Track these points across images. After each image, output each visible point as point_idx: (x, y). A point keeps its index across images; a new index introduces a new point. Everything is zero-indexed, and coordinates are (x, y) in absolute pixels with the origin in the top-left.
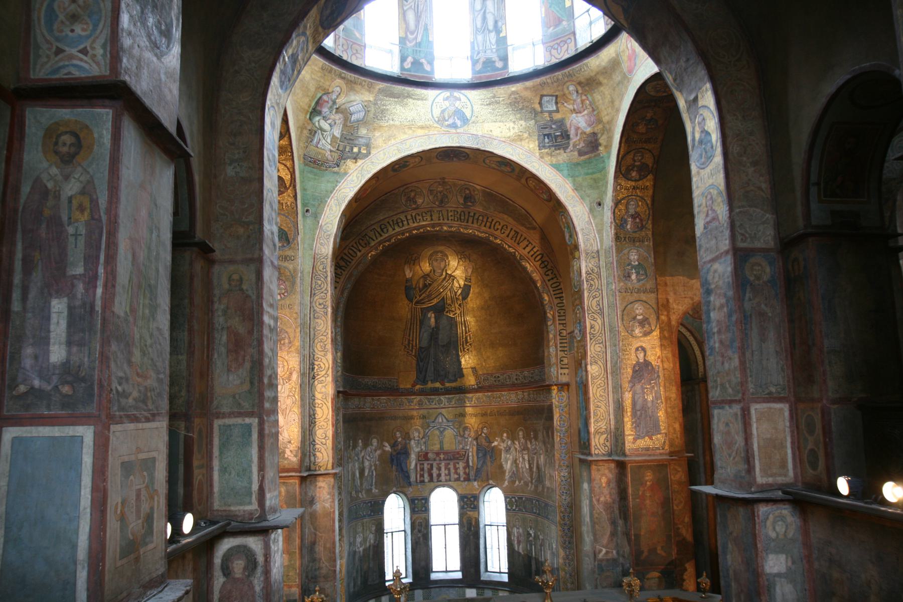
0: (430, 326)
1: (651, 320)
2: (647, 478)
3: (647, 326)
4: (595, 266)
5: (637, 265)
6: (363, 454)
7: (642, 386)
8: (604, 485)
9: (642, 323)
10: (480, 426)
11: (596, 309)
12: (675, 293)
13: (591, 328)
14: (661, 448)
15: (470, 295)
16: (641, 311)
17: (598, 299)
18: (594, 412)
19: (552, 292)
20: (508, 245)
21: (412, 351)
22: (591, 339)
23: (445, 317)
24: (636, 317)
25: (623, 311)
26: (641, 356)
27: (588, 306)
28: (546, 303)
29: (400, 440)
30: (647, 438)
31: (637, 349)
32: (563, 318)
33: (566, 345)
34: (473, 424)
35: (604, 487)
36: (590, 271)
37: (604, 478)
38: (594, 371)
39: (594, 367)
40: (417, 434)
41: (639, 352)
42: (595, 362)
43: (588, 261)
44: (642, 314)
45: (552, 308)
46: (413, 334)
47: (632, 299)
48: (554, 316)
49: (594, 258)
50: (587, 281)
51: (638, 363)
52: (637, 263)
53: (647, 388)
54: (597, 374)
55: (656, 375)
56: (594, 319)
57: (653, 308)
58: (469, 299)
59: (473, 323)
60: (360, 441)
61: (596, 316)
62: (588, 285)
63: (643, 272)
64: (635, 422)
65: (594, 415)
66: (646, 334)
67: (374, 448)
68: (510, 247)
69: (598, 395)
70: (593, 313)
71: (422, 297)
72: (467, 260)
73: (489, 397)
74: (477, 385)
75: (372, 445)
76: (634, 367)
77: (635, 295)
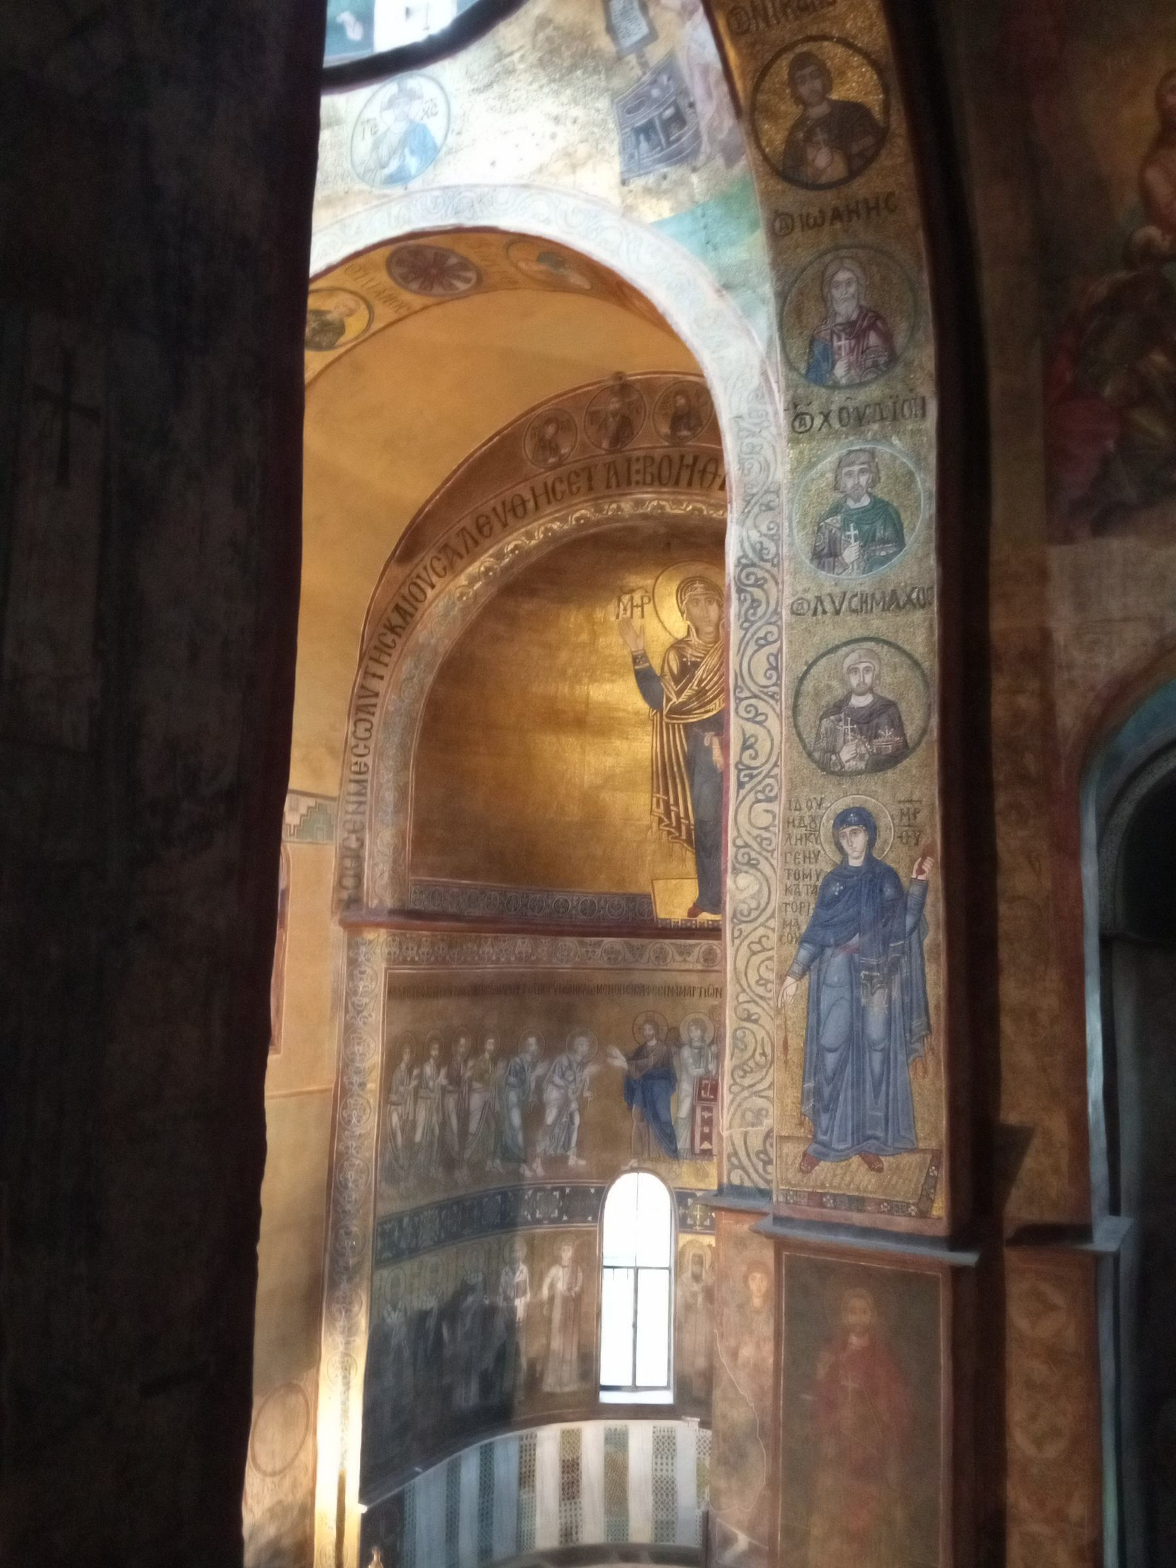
1: (903, 707)
2: (851, 1319)
3: (887, 734)
4: (771, 538)
5: (865, 510)
6: (540, 1070)
7: (851, 961)
8: (757, 1302)
9: (866, 723)
11: (764, 682)
12: (1081, 606)
13: (745, 747)
14: (913, 1209)
16: (868, 679)
17: (773, 648)
18: (734, 1036)
22: (741, 785)
24: (847, 698)
25: (802, 680)
26: (856, 844)
27: (739, 675)
29: (653, 1043)
30: (856, 1160)
31: (842, 820)
35: (758, 1312)
36: (751, 554)
37: (758, 1275)
38: (745, 894)
39: (744, 880)
40: (699, 1033)
41: (848, 830)
42: (748, 863)
43: (749, 522)
44: (871, 690)
47: (838, 635)
49: (769, 508)
50: (740, 591)
51: (841, 872)
52: (866, 501)
53: (870, 969)
54: (754, 904)
55: (910, 921)
56: (757, 718)
57: (916, 664)
60: (532, 1041)
61: (761, 706)
62: (741, 602)
63: (889, 533)
64: (817, 1093)
65: (735, 1046)
66: (881, 764)
67: (579, 1058)
69: (753, 977)
70: (755, 696)
75: (575, 1052)
76: (826, 884)
77: (852, 620)
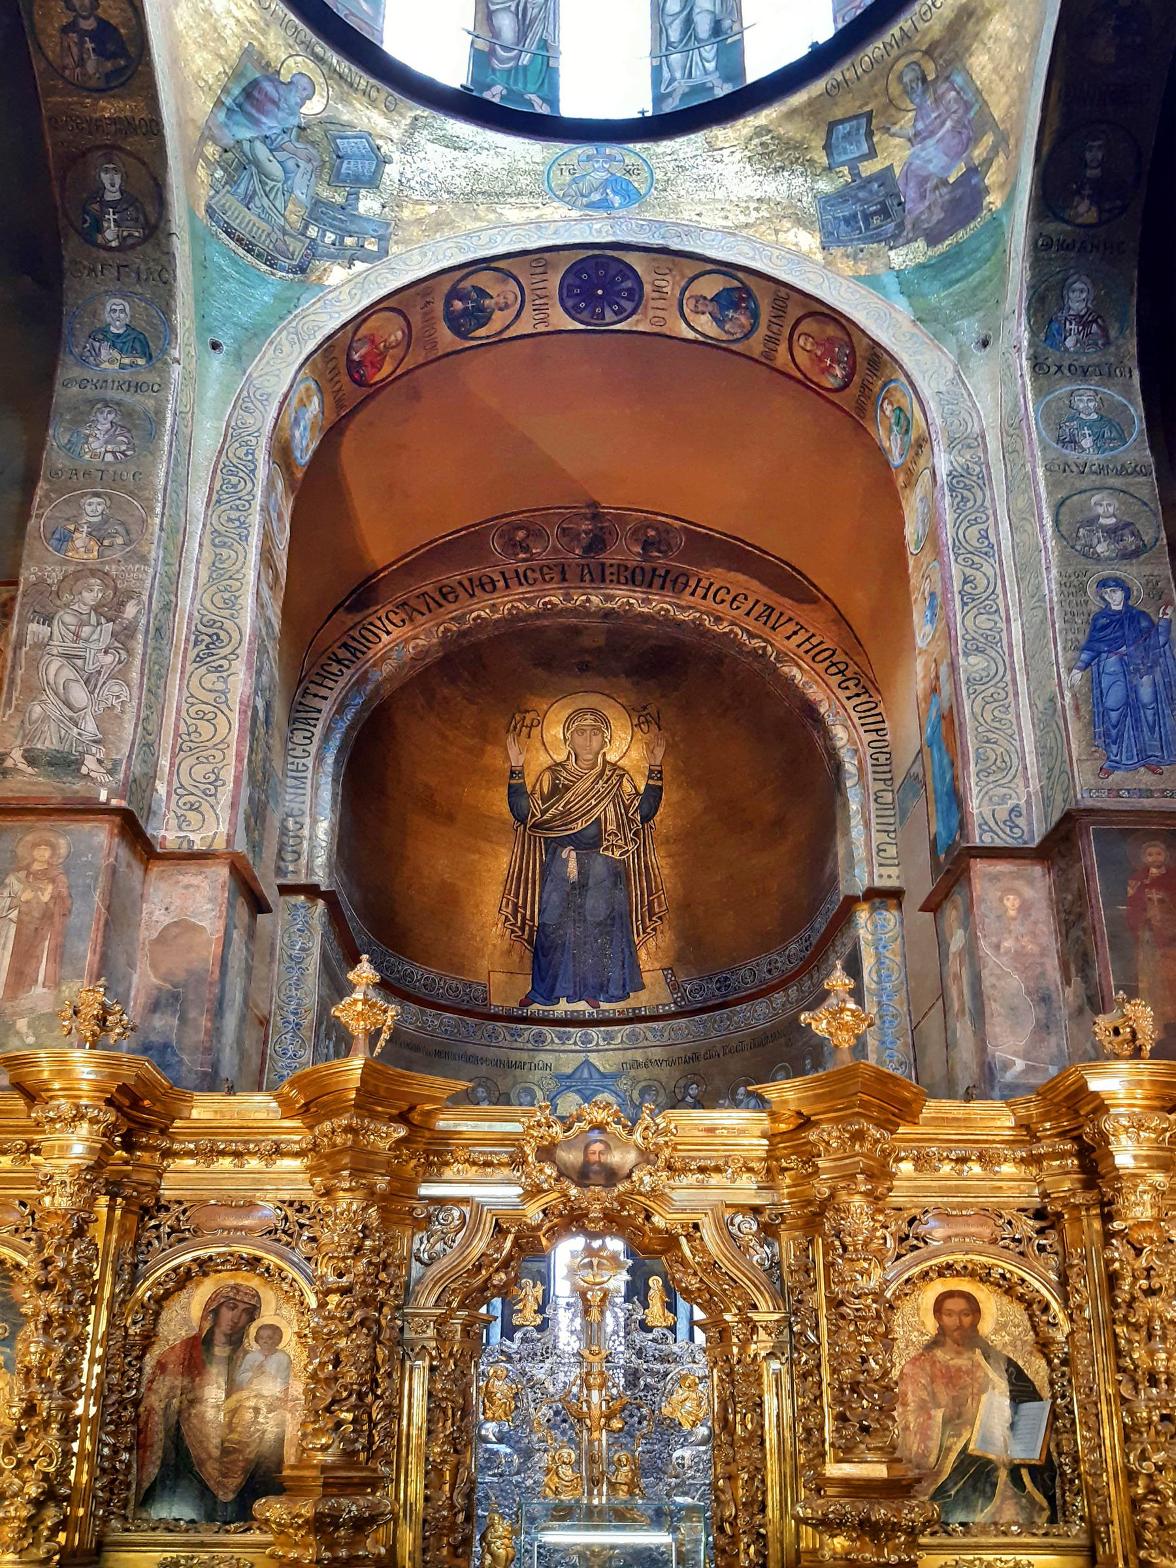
0: (566, 880)
10: (682, 1083)
15: (661, 810)
19: (856, 720)
20: (748, 632)
21: (522, 929)
23: (600, 860)
28: (839, 744)
32: (886, 768)
33: (892, 820)
34: (664, 1081)
45: (856, 751)
46: (526, 889)
48: (860, 769)
58: (657, 818)
59: (666, 871)
68: (751, 635)
71: (548, 816)
72: (654, 727)
73: (704, 1023)
74: (675, 1003)
